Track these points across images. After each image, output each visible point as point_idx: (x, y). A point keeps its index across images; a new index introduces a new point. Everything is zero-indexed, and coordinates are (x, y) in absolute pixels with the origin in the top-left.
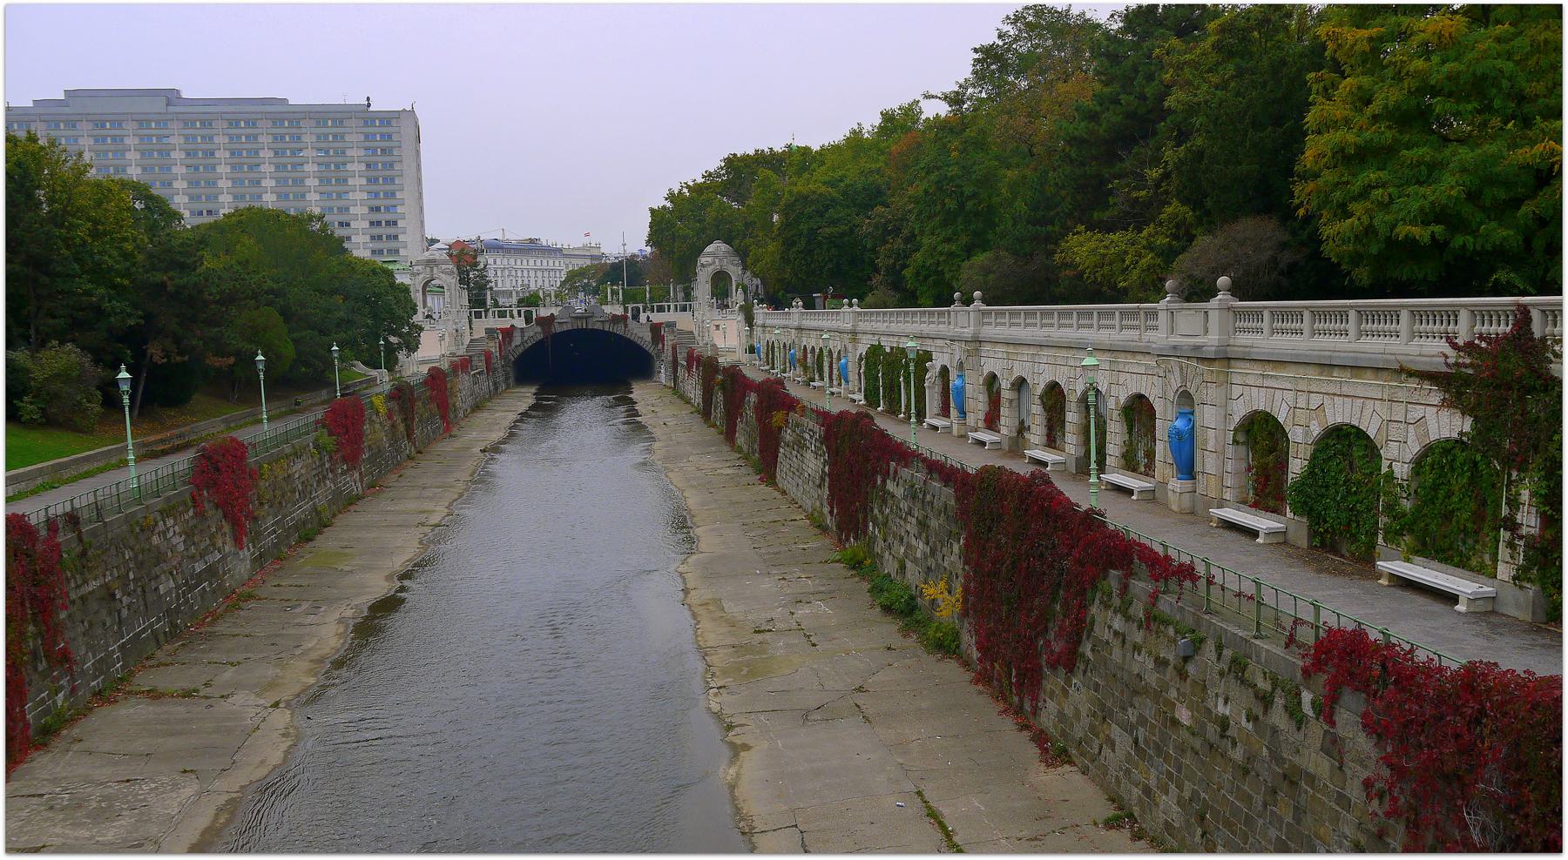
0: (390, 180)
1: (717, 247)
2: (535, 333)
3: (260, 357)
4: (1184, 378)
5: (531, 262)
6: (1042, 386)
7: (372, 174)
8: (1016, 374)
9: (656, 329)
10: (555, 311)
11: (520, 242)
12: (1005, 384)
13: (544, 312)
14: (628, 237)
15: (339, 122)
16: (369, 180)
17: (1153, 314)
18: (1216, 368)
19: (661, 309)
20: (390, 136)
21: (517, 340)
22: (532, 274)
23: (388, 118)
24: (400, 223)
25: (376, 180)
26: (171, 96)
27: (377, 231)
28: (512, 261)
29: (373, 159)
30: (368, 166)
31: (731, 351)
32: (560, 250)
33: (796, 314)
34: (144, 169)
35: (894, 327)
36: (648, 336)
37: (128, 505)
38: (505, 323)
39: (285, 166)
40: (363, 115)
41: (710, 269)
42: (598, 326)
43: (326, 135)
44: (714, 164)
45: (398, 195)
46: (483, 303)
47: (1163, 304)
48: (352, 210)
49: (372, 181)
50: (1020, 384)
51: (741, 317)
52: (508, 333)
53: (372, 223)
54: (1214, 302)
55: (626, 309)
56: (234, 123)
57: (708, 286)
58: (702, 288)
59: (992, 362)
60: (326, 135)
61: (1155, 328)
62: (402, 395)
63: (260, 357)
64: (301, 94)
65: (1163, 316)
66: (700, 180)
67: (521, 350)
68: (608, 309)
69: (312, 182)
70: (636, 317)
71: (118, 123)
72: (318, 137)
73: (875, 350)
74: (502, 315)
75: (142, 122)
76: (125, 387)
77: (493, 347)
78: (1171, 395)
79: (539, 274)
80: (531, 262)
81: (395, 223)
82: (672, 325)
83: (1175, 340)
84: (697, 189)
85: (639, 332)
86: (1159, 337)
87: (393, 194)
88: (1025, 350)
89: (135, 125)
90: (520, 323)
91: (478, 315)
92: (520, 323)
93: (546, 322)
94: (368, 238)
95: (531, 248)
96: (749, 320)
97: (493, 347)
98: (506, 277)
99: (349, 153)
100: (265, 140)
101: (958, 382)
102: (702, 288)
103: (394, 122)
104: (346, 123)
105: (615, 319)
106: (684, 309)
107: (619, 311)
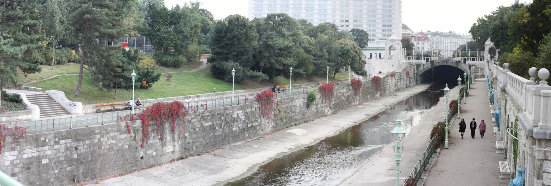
0: (390, 11)
2: (428, 66)
5: (449, 40)
9: (470, 67)
10: (437, 58)
11: (446, 33)
13: (433, 59)
16: (383, 11)
19: (474, 60)
21: (422, 68)
22: (449, 44)
25: (386, 11)
27: (384, 28)
28: (442, 39)
30: (383, 6)
32: (460, 36)
37: (234, 104)
42: (450, 64)
45: (393, 16)
49: (384, 11)
52: (418, 66)
53: (383, 26)
55: (462, 59)
62: (356, 85)
66: (491, 14)
70: (465, 62)
74: (418, 59)
79: (452, 44)
80: (449, 40)
81: (391, 26)
84: (489, 17)
92: (423, 62)
93: (432, 62)
94: (382, 31)
95: (450, 35)
105: (458, 62)
106: (481, 60)
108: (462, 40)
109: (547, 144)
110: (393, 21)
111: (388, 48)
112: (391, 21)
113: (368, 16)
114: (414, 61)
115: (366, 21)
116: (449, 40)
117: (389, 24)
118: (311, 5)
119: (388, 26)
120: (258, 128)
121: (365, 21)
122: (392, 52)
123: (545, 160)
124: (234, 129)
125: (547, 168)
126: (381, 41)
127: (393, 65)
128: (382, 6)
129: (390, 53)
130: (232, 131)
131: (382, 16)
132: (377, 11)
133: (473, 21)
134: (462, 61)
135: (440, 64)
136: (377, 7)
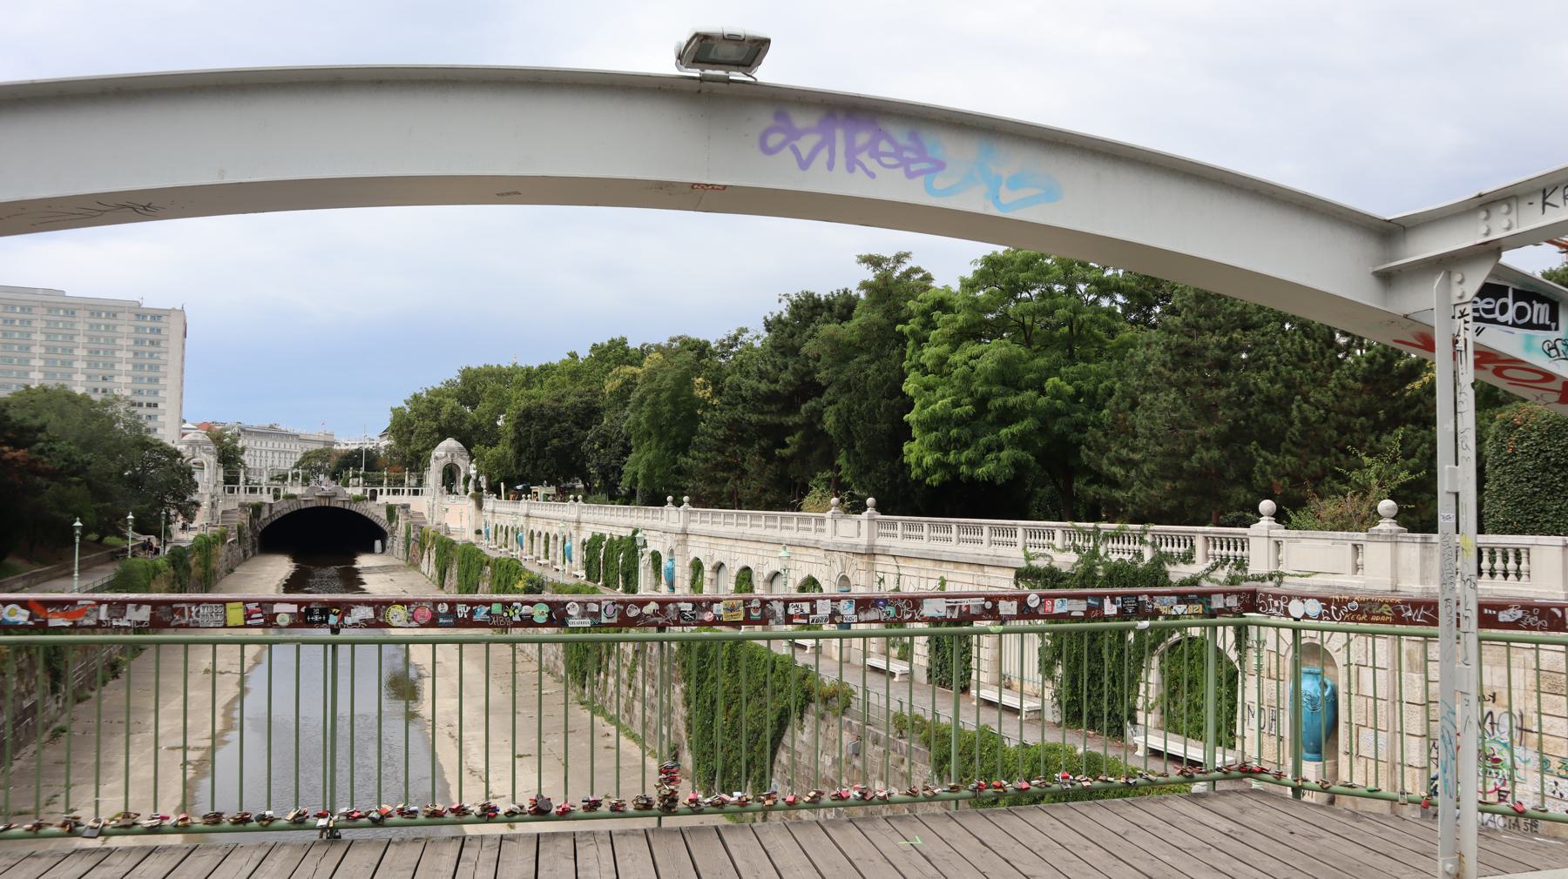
1: (450, 443)
3: (78, 524)
4: (844, 567)
6: (737, 569)
7: (139, 361)
8: (717, 559)
9: (391, 510)
12: (707, 568)
16: (135, 366)
17: (822, 520)
18: (865, 559)
19: (395, 492)
20: (159, 331)
21: (265, 514)
23: (157, 315)
25: (142, 366)
29: (140, 348)
30: (136, 354)
31: (463, 531)
33: (523, 506)
34: (46, 374)
35: (614, 520)
36: (384, 515)
39: (55, 349)
41: (443, 462)
42: (340, 505)
43: (99, 326)
44: (453, 375)
45: (161, 381)
46: (236, 481)
47: (829, 514)
50: (719, 567)
51: (472, 503)
52: (257, 509)
54: (865, 515)
57: (440, 476)
58: (433, 476)
59: (697, 549)
60: (99, 326)
61: (823, 531)
63: (78, 524)
65: (829, 524)
68: (349, 491)
70: (373, 498)
72: (91, 326)
73: (597, 540)
77: (243, 519)
78: (834, 578)
81: (156, 405)
82: (406, 507)
83: (837, 539)
85: (375, 512)
86: (826, 537)
88: (724, 542)
90: (267, 498)
95: (271, 433)
96: (480, 506)
98: (260, 459)
99: (118, 341)
100: (38, 325)
101: (669, 564)
102: (433, 476)
103: (164, 319)
104: (119, 316)
105: (357, 499)
106: (416, 493)
107: (358, 491)
110: (161, 394)
112: (156, 393)
113: (89, 377)
114: (243, 496)
116: (270, 444)
117: (152, 400)
119: (149, 405)
128: (131, 355)
131: (129, 380)
132: (117, 367)
136: (118, 354)
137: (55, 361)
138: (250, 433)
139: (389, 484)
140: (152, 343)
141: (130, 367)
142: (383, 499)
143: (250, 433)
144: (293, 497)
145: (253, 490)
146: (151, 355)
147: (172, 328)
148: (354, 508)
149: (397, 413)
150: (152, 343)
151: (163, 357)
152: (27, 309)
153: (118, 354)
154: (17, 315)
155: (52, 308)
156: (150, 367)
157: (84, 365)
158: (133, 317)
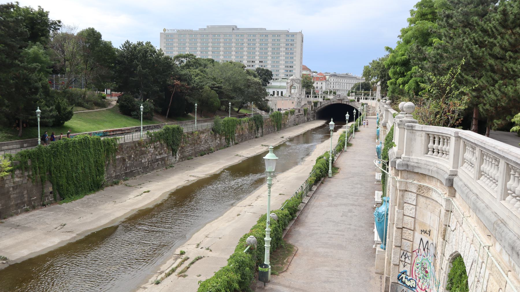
5: (346, 81)
9: (363, 105)
14: (358, 74)
15: (279, 35)
16: (286, 53)
19: (366, 99)
20: (293, 40)
21: (319, 105)
22: (346, 84)
23: (293, 35)
24: (294, 67)
25: (288, 53)
26: (234, 28)
27: (287, 69)
28: (339, 80)
38: (315, 100)
40: (287, 34)
42: (345, 103)
45: (294, 58)
48: (280, 62)
52: (316, 104)
56: (249, 35)
60: (275, 40)
64: (271, 27)
67: (320, 108)
69: (269, 53)
71: (219, 35)
75: (225, 34)
76: (142, 110)
77: (309, 107)
79: (348, 85)
80: (346, 81)
87: (293, 58)
89: (223, 36)
90: (320, 100)
91: (308, 97)
95: (346, 76)
97: (309, 107)
99: (281, 45)
103: (295, 36)
108: (358, 81)
109: (409, 176)
110: (294, 63)
111: (289, 87)
112: (293, 62)
113: (272, 57)
114: (312, 99)
115: (271, 62)
117: (291, 65)
118: (183, 39)
120: (166, 159)
121: (269, 62)
122: (293, 91)
123: (406, 191)
124: (143, 161)
125: (408, 199)
126: (283, 80)
127: (293, 103)
128: (285, 49)
129: (291, 92)
130: (142, 163)
131: (284, 58)
132: (281, 54)
133: (367, 62)
134: (356, 100)
135: (336, 103)
137: (262, 52)
138: (338, 76)
139: (364, 95)
140: (291, 45)
141: (284, 54)
142: (362, 101)
143: (338, 76)
144: (329, 99)
145: (316, 97)
146: (291, 49)
147: (298, 39)
148: (350, 104)
149: (366, 68)
150: (291, 45)
151: (295, 49)
152: (254, 35)
153: (281, 49)
154: (252, 38)
155: (261, 35)
156: (291, 53)
157: (271, 53)
158: (285, 36)
